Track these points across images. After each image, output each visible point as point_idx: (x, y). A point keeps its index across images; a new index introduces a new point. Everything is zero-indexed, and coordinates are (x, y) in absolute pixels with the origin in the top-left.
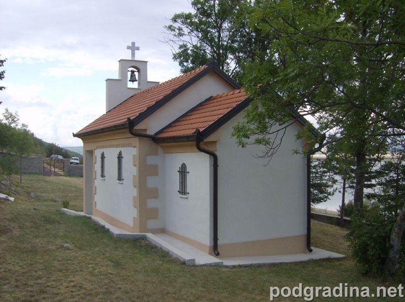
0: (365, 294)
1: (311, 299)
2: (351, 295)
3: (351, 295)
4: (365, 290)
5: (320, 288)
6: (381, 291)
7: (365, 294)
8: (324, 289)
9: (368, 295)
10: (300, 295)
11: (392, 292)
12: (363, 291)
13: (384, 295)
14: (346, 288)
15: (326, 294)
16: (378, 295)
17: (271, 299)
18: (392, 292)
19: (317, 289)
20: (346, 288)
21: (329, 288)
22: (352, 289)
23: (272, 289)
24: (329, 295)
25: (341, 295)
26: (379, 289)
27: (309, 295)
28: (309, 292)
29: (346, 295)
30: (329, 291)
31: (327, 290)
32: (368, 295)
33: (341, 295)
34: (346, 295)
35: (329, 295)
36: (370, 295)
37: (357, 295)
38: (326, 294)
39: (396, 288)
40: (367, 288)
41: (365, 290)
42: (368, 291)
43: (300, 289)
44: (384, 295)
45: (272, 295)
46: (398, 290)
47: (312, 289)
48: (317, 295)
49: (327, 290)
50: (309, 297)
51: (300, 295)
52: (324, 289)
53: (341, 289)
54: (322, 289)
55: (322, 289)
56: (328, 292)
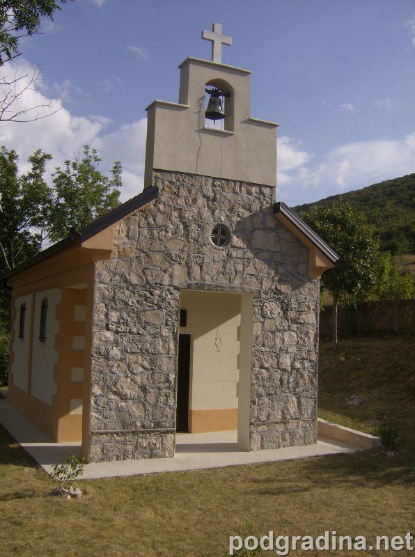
8: (304, 539)
10: (271, 547)
12: (357, 541)
13: (387, 548)
14: (334, 538)
15: (307, 545)
20: (334, 538)
21: (310, 538)
23: (232, 539)
24: (311, 547)
25: (326, 547)
27: (282, 548)
28: (283, 543)
29: (334, 548)
30: (311, 542)
32: (364, 547)
35: (311, 547)
36: (367, 548)
37: (350, 548)
38: (307, 545)
44: (387, 548)
48: (294, 548)
49: (307, 540)
50: (283, 550)
51: (271, 547)
52: (304, 539)
54: (301, 538)
56: (308, 544)
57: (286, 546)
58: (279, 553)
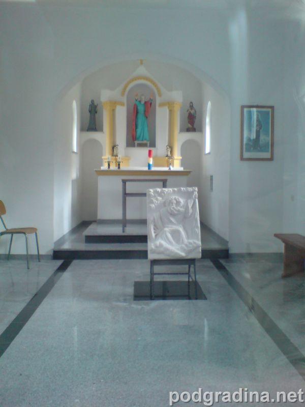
0: (265, 399)
1: (211, 404)
2: (251, 400)
3: (251, 400)
4: (264, 395)
5: (220, 393)
6: (281, 395)
7: (265, 399)
8: (224, 394)
9: (267, 400)
10: (199, 400)
11: (292, 397)
13: (284, 400)
15: (226, 399)
16: (278, 400)
17: (171, 404)
18: (292, 397)
19: (217, 394)
20: (246, 393)
22: (251, 394)
24: (229, 400)
25: (240, 400)
26: (278, 394)
27: (209, 400)
29: (246, 400)
30: (229, 396)
31: (226, 395)
32: (267, 400)
33: (240, 400)
34: (246, 400)
35: (229, 400)
37: (257, 400)
38: (226, 399)
39: (297, 393)
40: (267, 393)
41: (264, 395)
42: (267, 396)
43: (200, 393)
44: (284, 400)
45: (171, 400)
46: (298, 396)
47: (211, 393)
48: (216, 400)
49: (226, 395)
50: (209, 402)
51: (199, 400)
53: (240, 393)
54: (222, 394)
55: (222, 394)
56: (227, 397)
57: (211, 399)
58: (205, 404)
